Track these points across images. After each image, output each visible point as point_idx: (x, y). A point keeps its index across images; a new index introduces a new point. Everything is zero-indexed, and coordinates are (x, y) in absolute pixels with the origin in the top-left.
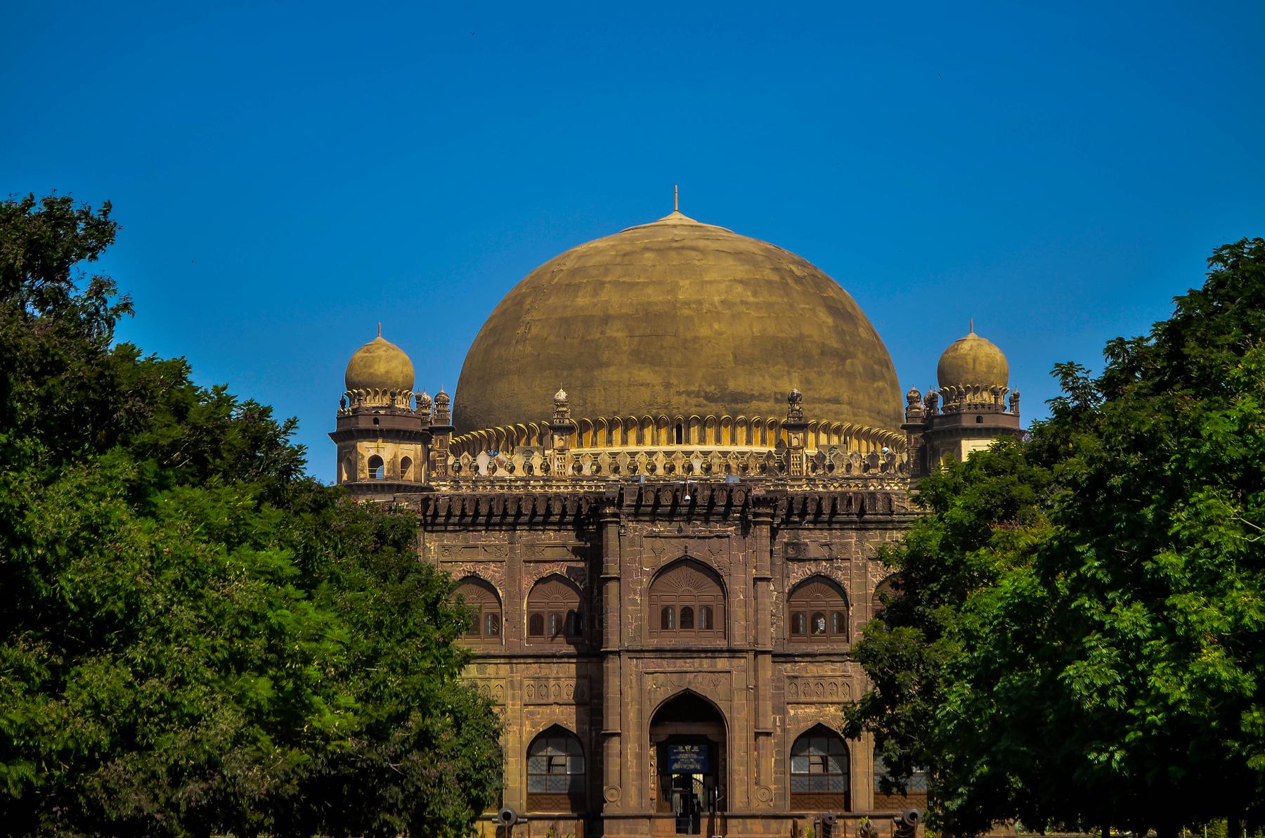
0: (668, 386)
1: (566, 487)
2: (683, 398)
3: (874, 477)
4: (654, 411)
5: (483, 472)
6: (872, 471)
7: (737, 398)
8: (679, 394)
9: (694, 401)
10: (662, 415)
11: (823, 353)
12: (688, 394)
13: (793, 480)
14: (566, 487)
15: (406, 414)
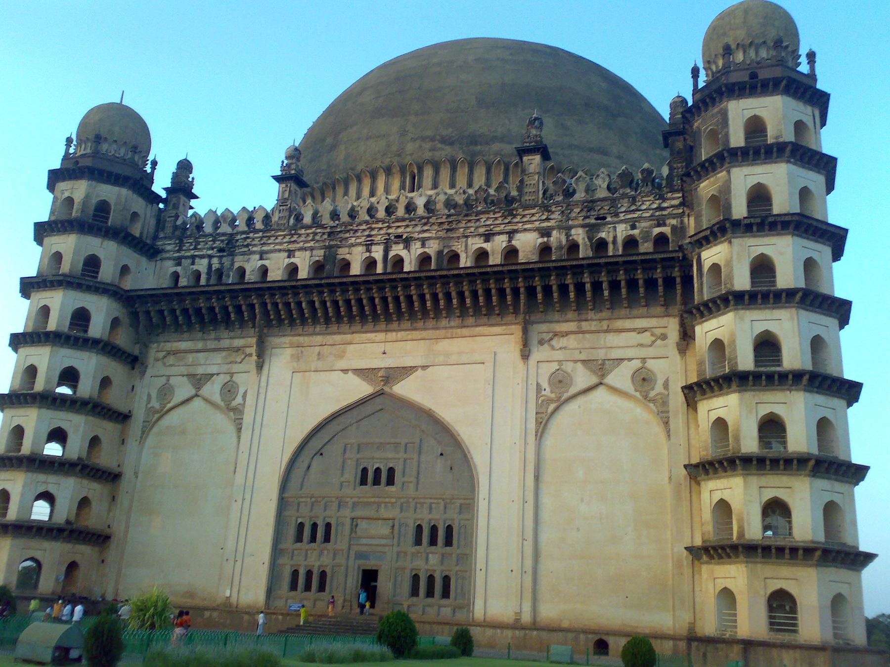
0: (403, 133)
1: (285, 236)
2: (418, 143)
3: (624, 196)
4: (387, 161)
5: (208, 228)
6: (621, 191)
7: (474, 140)
8: (414, 140)
9: (427, 145)
10: (395, 160)
11: (587, 105)
12: (423, 139)
13: (526, 207)
14: (285, 236)
15: (114, 160)
